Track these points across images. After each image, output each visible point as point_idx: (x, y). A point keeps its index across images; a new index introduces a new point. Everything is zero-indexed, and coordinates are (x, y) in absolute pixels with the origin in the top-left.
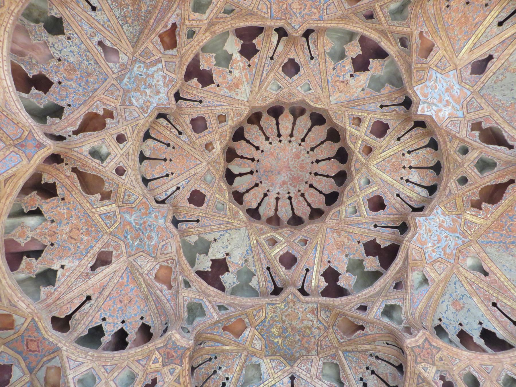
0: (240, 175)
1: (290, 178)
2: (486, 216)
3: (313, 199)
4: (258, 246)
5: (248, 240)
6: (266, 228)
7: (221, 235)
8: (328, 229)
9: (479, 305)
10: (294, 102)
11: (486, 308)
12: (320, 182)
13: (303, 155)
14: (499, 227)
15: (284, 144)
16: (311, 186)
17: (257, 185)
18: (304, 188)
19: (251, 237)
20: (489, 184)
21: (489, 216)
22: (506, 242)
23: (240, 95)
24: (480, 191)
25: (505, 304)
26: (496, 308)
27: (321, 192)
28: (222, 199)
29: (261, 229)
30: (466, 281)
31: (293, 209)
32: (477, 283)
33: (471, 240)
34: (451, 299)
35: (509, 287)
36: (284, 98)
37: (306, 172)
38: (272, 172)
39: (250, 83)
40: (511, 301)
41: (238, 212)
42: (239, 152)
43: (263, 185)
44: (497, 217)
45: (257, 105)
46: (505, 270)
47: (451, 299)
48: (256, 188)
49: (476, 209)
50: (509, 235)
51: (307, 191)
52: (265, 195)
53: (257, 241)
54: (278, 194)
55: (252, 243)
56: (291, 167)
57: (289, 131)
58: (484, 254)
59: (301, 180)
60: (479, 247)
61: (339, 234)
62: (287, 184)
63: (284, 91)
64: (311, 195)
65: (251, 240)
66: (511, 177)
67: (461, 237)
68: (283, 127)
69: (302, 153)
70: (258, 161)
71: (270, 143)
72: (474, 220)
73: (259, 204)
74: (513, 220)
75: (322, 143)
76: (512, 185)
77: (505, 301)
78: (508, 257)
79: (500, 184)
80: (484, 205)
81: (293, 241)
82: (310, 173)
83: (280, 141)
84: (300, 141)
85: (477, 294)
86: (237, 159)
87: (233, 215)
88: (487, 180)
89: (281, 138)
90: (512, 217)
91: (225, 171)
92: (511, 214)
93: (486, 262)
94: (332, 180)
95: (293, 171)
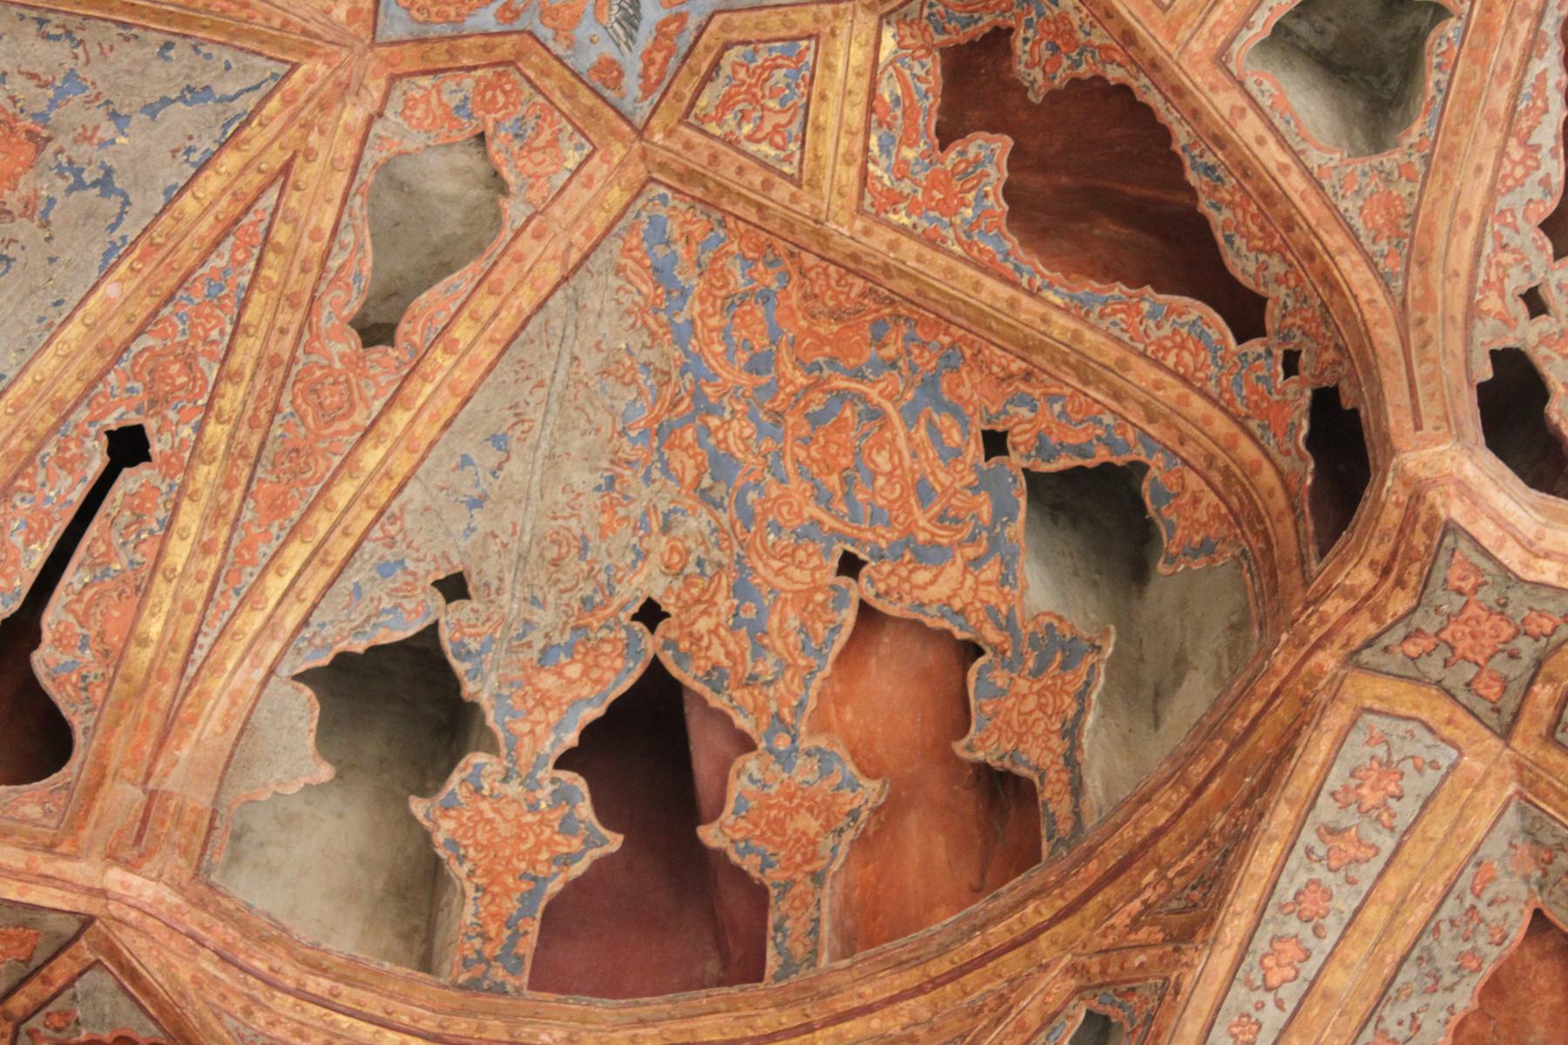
2: (894, 199)
9: (74, 331)
11: (69, 388)
14: (827, 328)
20: (1182, 134)
21: (902, 218)
22: (710, 411)
24: (1101, 79)
25: (168, 525)
26: (98, 463)
30: (256, 179)
32: (271, 273)
33: (641, 132)
34: (39, 99)
35: (322, 522)
40: (211, 564)
44: (905, 287)
46: (466, 461)
47: (39, 99)
49: (932, 102)
50: (777, 416)
58: (554, 273)
60: (600, 220)
66: (1278, 295)
67: (645, 36)
72: (828, 115)
74: (911, 416)
76: (1217, 327)
77: (190, 516)
78: (587, 457)
79: (1203, 224)
80: (989, 152)
85: (169, 298)
88: (1223, 102)
90: (941, 406)
92: (965, 391)
93: (486, 304)
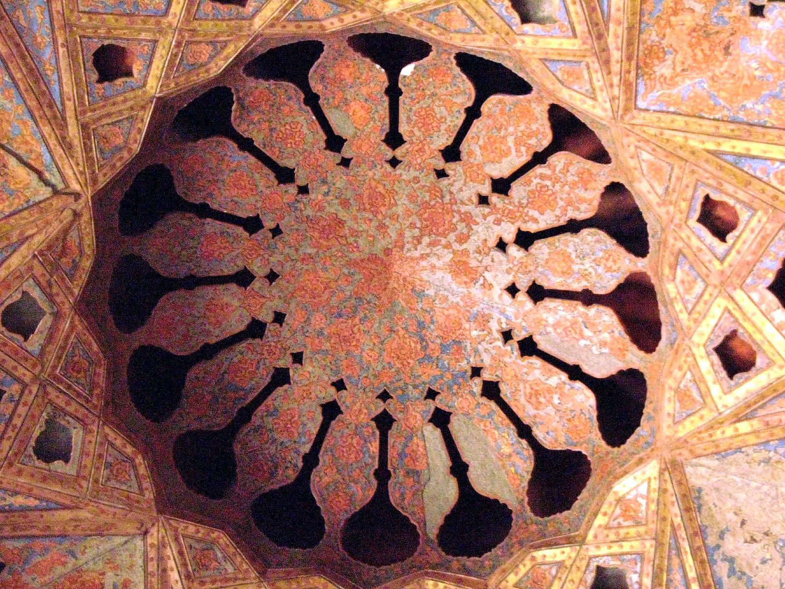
0: (459, 469)
1: (432, 244)
3: (510, 141)
4: (761, 412)
5: (739, 456)
6: (677, 373)
7: (732, 572)
8: (641, 104)
10: (99, 341)
12: (426, 120)
13: (321, 209)
15: (287, 302)
16: (452, 153)
17: (491, 390)
18: (464, 184)
19: (723, 447)
23: (125, 575)
27: (473, 113)
28: (576, 576)
29: (682, 396)
31: (574, 227)
36: (93, 385)
37: (399, 179)
38: (421, 325)
39: (66, 544)
41: (619, 501)
42: (363, 492)
43: (487, 360)
45: (149, 495)
48: (505, 391)
51: (480, 166)
52: (528, 347)
53: (738, 418)
54: (512, 290)
55: (752, 440)
56: (382, 243)
57: (230, 295)
59: (433, 197)
61: (656, 53)
62: (465, 252)
63: (61, 401)
64: (496, 152)
65: (737, 442)
68: (218, 323)
69: (309, 212)
70: (384, 396)
71: (298, 358)
73: (575, 373)
75: (246, 145)
81: (722, 260)
82: (394, 162)
83: (279, 318)
84: (259, 235)
86: (394, 497)
87: (638, 524)
89: (266, 316)
91: (456, 562)
94: (407, 71)
95: (401, 235)
